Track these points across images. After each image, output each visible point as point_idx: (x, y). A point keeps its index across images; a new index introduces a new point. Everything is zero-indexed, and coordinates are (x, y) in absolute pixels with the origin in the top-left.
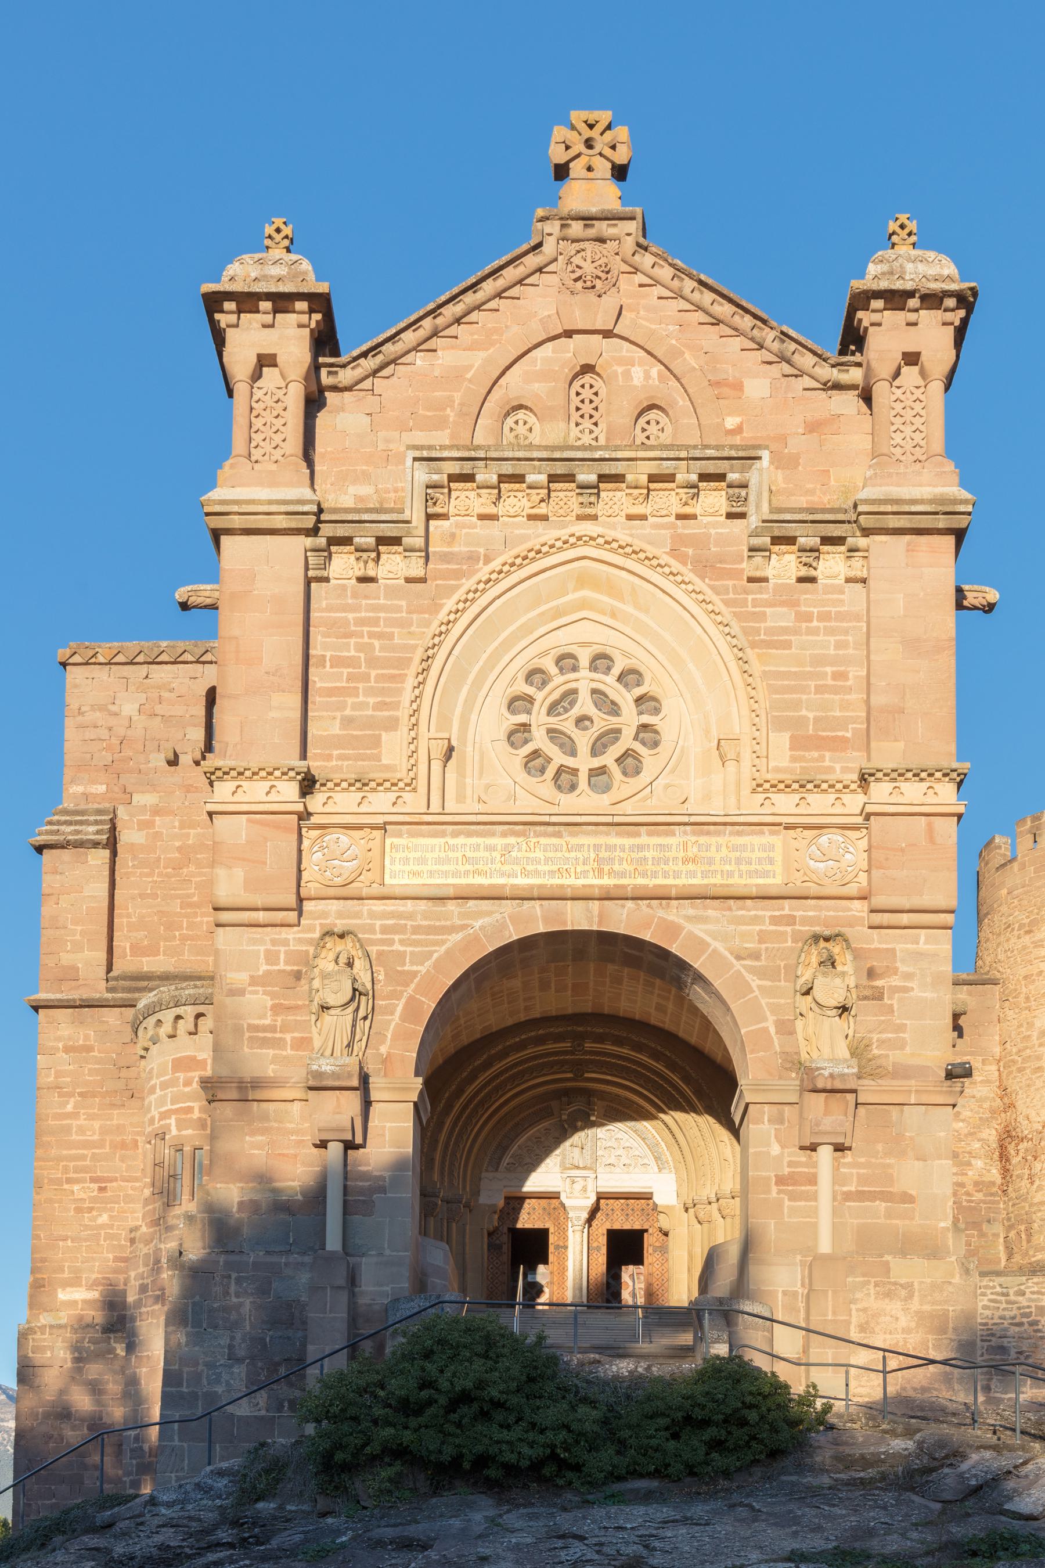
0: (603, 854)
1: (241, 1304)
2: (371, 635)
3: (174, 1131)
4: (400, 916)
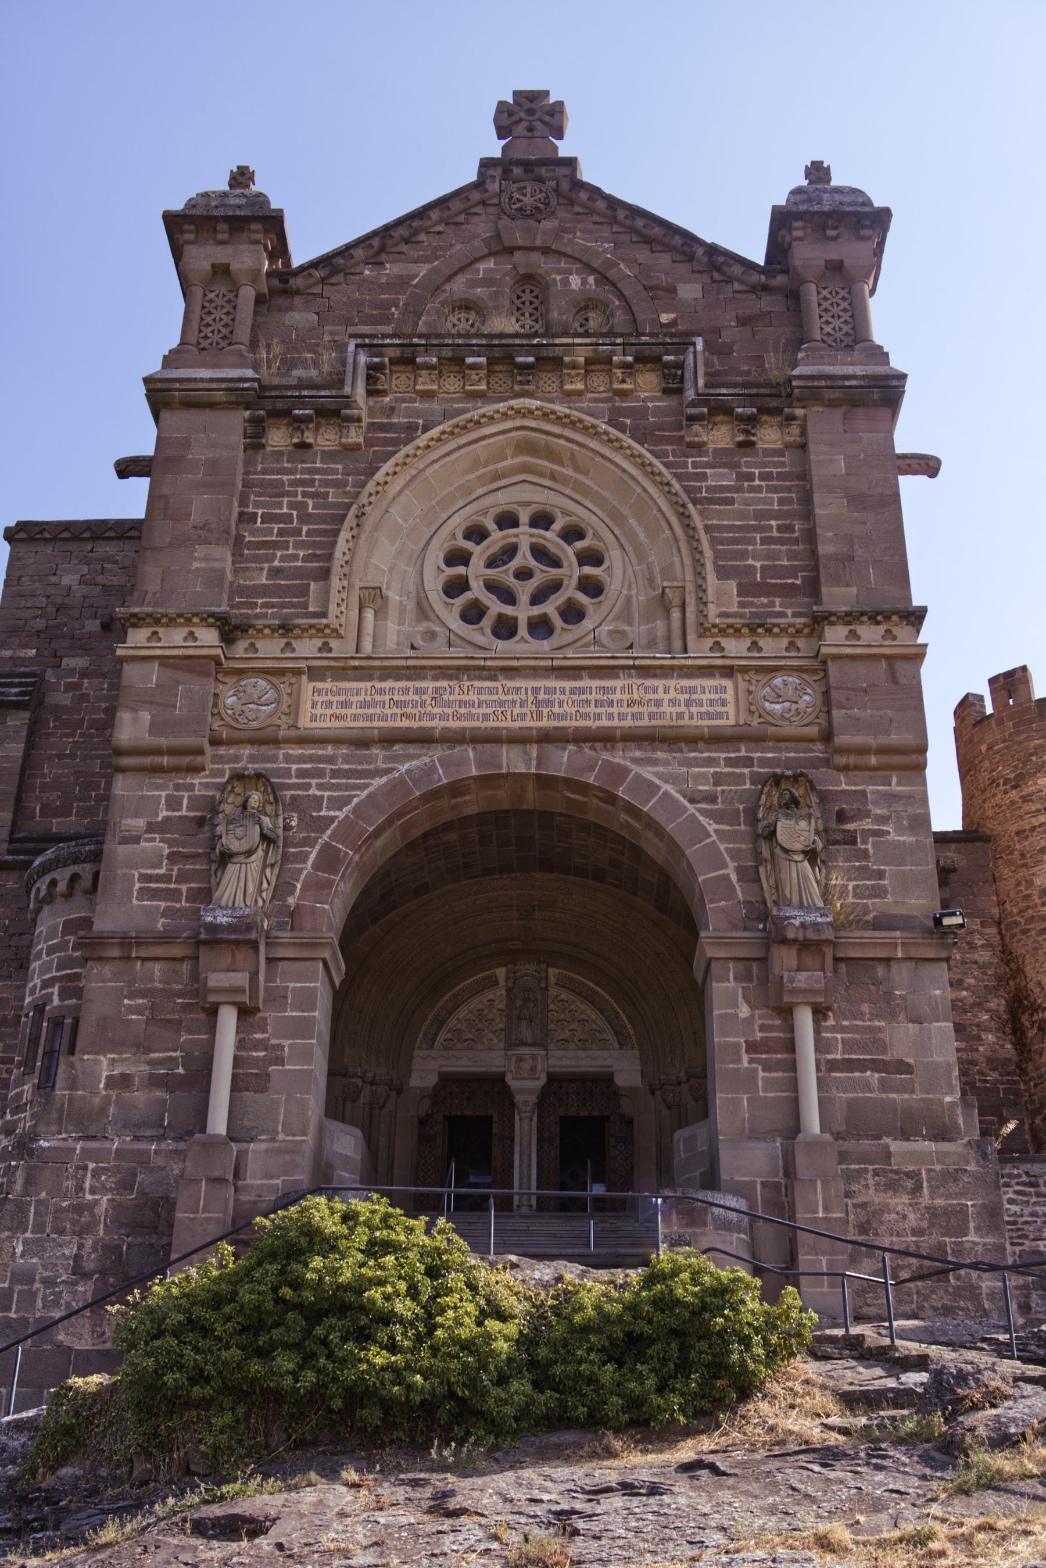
0: (541, 696)
1: (96, 1202)
2: (305, 494)
3: (56, 1001)
4: (319, 759)
